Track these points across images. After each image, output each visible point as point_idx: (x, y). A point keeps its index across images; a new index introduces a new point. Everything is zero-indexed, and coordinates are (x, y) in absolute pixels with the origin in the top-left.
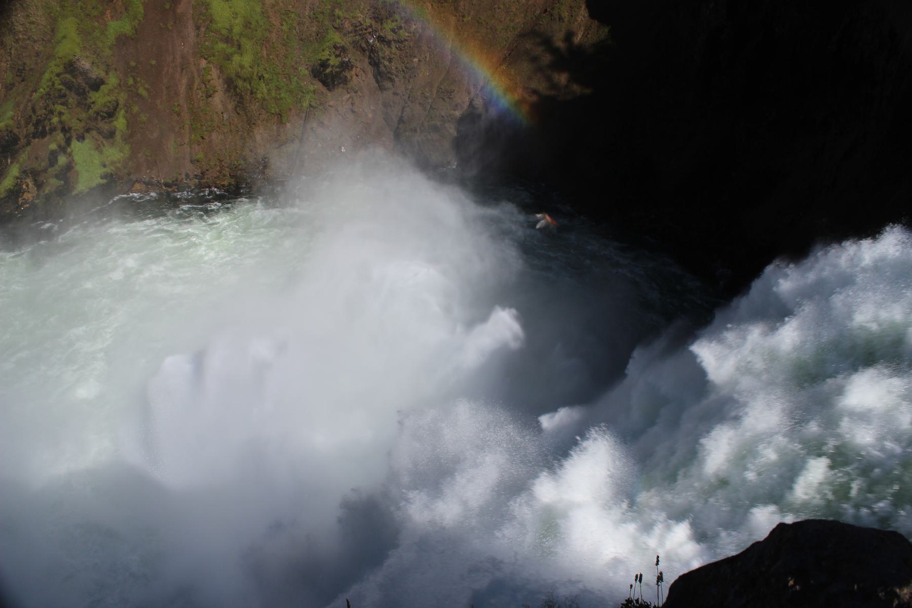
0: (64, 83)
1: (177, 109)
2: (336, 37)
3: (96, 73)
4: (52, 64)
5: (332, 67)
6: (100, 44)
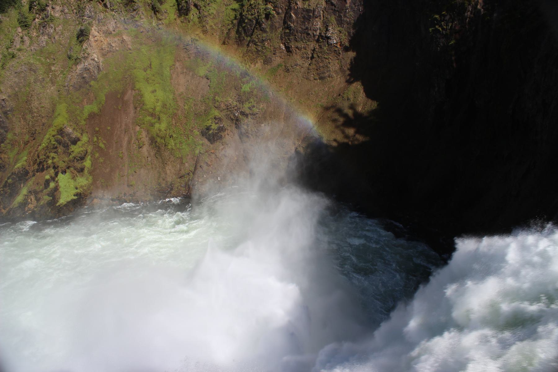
0: (56, 141)
1: (121, 155)
2: (216, 113)
3: (76, 134)
4: (51, 129)
5: (213, 130)
6: (79, 118)
